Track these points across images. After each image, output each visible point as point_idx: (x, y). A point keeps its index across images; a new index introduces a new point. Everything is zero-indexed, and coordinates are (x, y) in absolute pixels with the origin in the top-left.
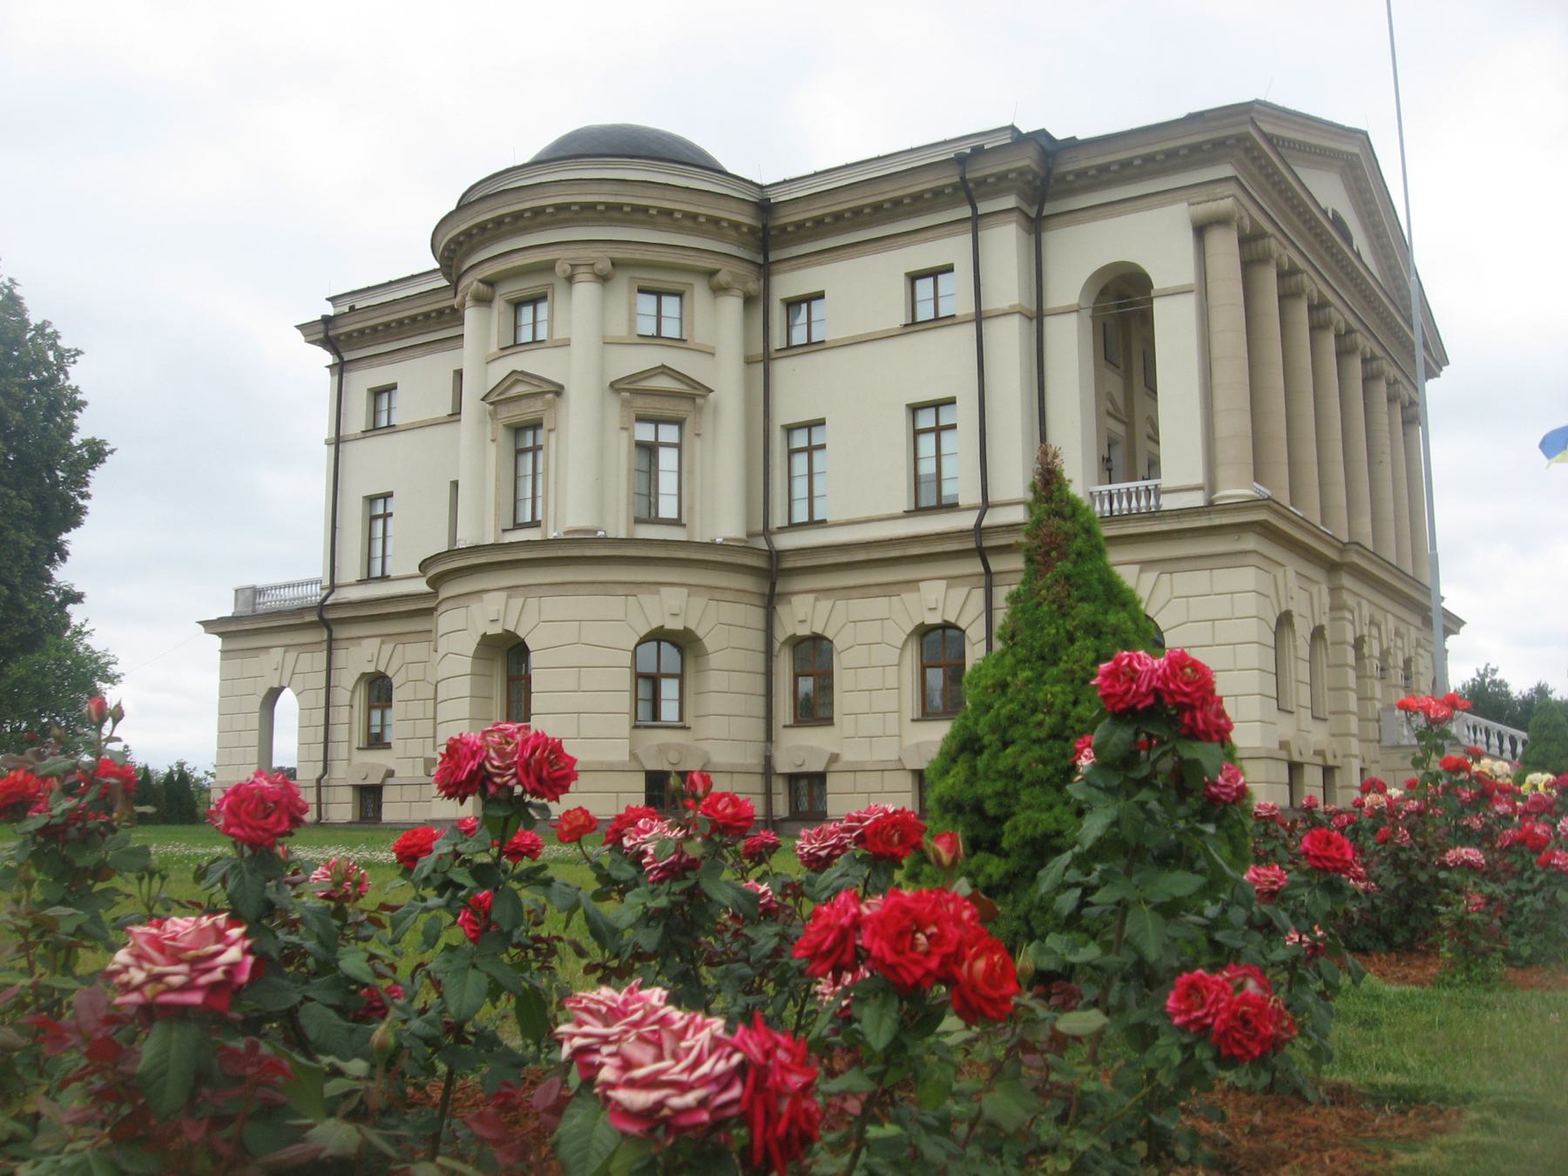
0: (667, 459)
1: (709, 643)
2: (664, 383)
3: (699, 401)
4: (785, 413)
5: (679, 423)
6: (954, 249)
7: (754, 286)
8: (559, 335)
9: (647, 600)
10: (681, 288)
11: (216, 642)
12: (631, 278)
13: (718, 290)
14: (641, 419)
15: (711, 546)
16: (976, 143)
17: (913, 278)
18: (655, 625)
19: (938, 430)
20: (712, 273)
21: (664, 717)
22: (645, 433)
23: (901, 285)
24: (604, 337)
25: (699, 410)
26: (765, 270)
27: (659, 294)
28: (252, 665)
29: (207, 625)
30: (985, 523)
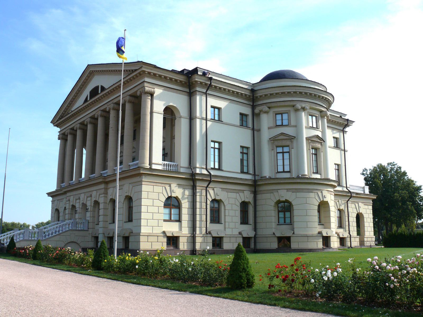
0: (286, 156)
1: (293, 203)
2: (282, 137)
3: (292, 140)
5: (288, 146)
9: (275, 194)
10: (287, 112)
12: (273, 111)
13: (297, 110)
14: (277, 147)
15: (298, 177)
18: (278, 199)
20: (294, 106)
21: (286, 222)
22: (280, 150)
24: (268, 127)
27: (282, 114)
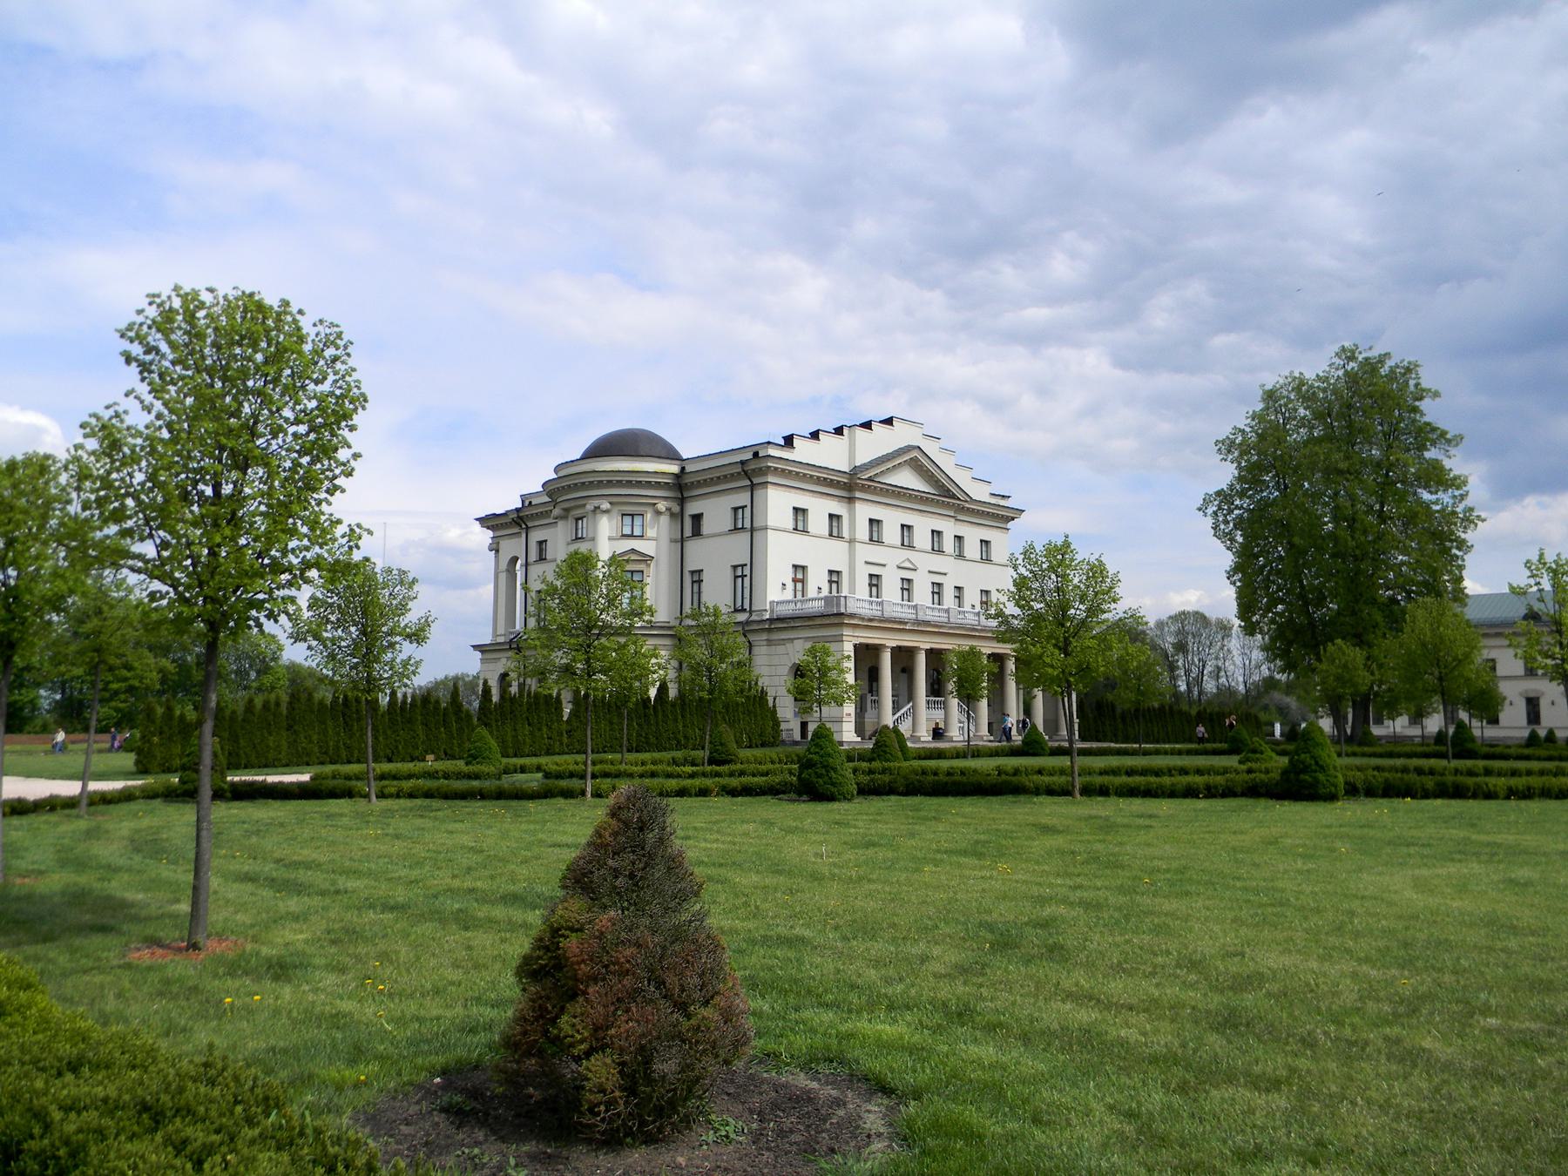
2: (634, 557)
4: (691, 565)
6: (742, 499)
7: (676, 509)
8: (590, 535)
11: (478, 655)
13: (658, 513)
16: (755, 449)
17: (735, 509)
19: (743, 576)
23: (729, 515)
25: (649, 566)
26: (682, 501)
28: (491, 666)
29: (475, 647)
30: (752, 618)
